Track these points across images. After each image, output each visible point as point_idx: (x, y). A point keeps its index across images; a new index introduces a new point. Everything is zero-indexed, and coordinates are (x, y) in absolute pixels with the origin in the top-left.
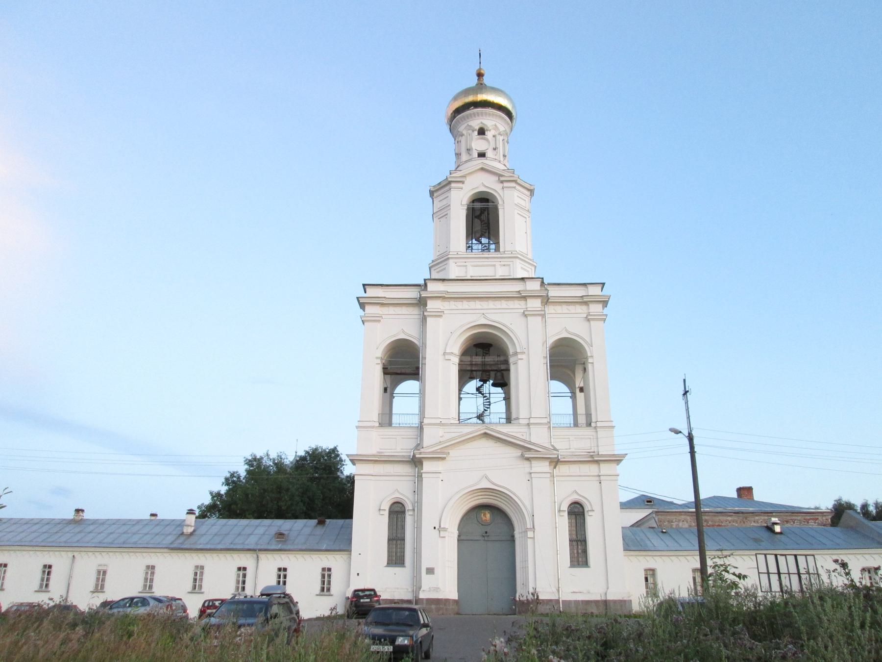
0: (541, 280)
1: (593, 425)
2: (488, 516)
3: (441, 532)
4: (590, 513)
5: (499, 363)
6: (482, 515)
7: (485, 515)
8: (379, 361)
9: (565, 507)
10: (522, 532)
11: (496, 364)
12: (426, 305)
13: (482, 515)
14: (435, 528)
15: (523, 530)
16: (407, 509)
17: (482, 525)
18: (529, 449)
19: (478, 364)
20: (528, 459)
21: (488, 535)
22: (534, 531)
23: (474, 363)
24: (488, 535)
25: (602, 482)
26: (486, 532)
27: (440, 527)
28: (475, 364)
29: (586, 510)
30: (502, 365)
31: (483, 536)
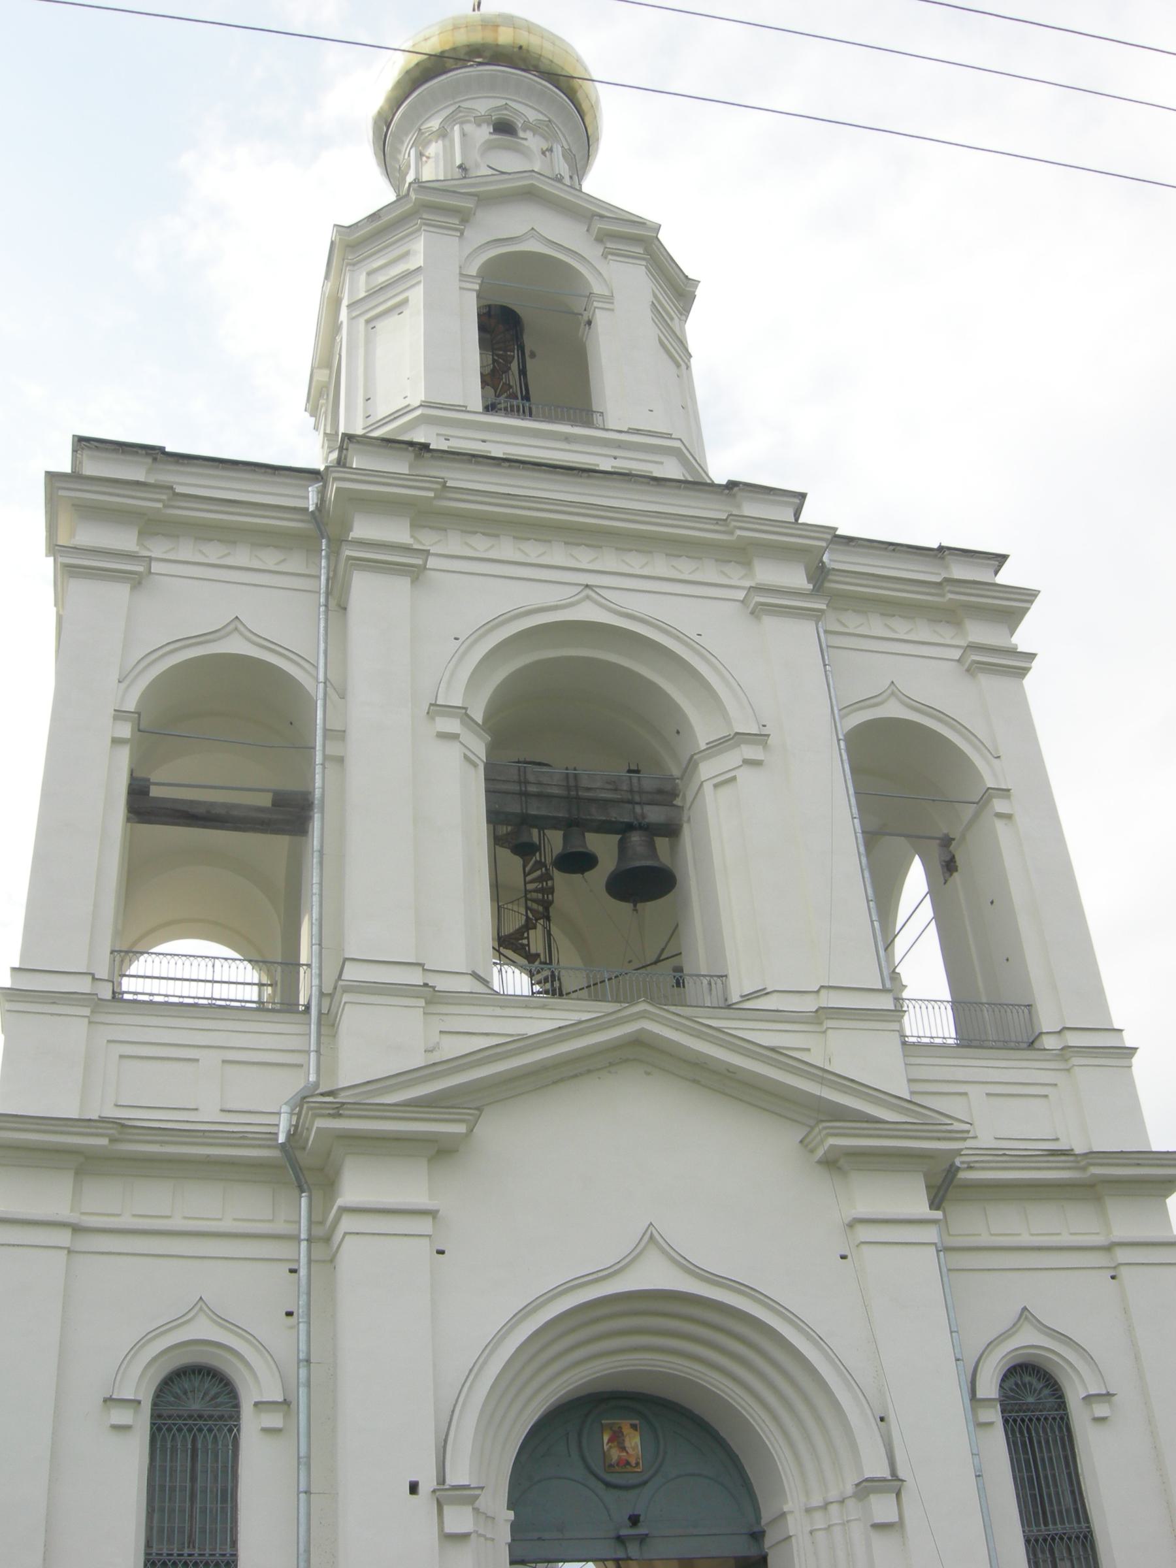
0: (797, 501)
1: (1049, 1042)
2: (633, 1441)
3: (446, 1509)
4: (1101, 1410)
5: (637, 798)
6: (606, 1438)
7: (617, 1438)
8: (125, 730)
9: (989, 1387)
10: (825, 1507)
11: (622, 801)
12: (338, 542)
13: (606, 1438)
14: (414, 1488)
15: (833, 1495)
16: (248, 1397)
17: (608, 1485)
18: (839, 1114)
19: (550, 796)
20: (834, 1163)
21: (641, 1530)
22: (898, 1494)
23: (532, 789)
24: (641, 1530)
25: (1124, 1272)
26: (634, 1520)
27: (442, 1480)
28: (539, 796)
29: (1074, 1397)
30: (647, 808)
31: (620, 1540)
